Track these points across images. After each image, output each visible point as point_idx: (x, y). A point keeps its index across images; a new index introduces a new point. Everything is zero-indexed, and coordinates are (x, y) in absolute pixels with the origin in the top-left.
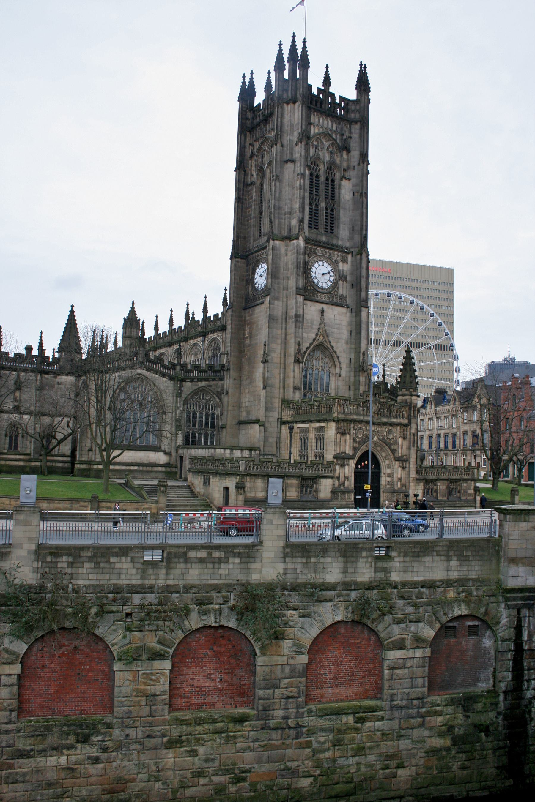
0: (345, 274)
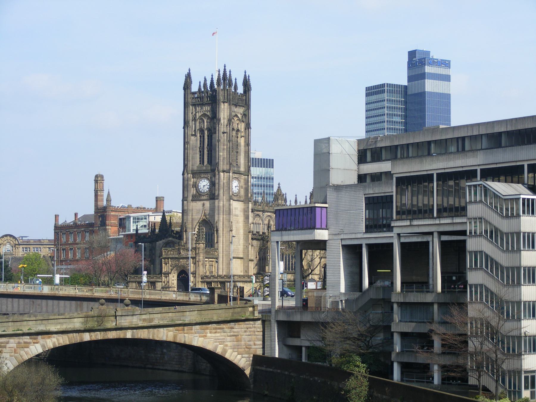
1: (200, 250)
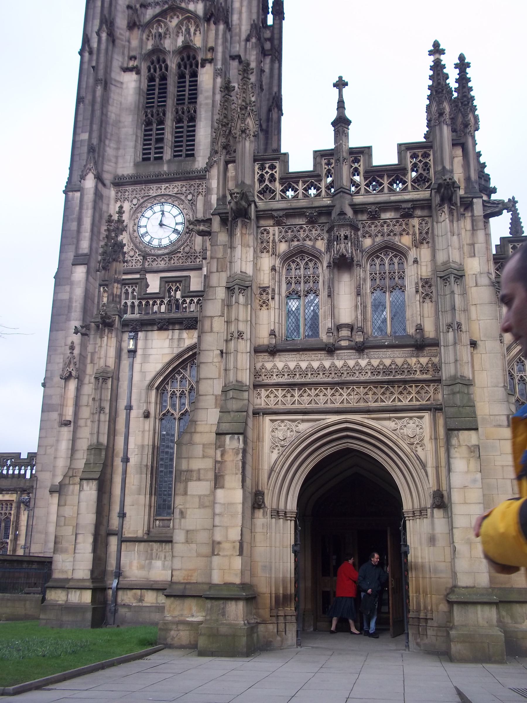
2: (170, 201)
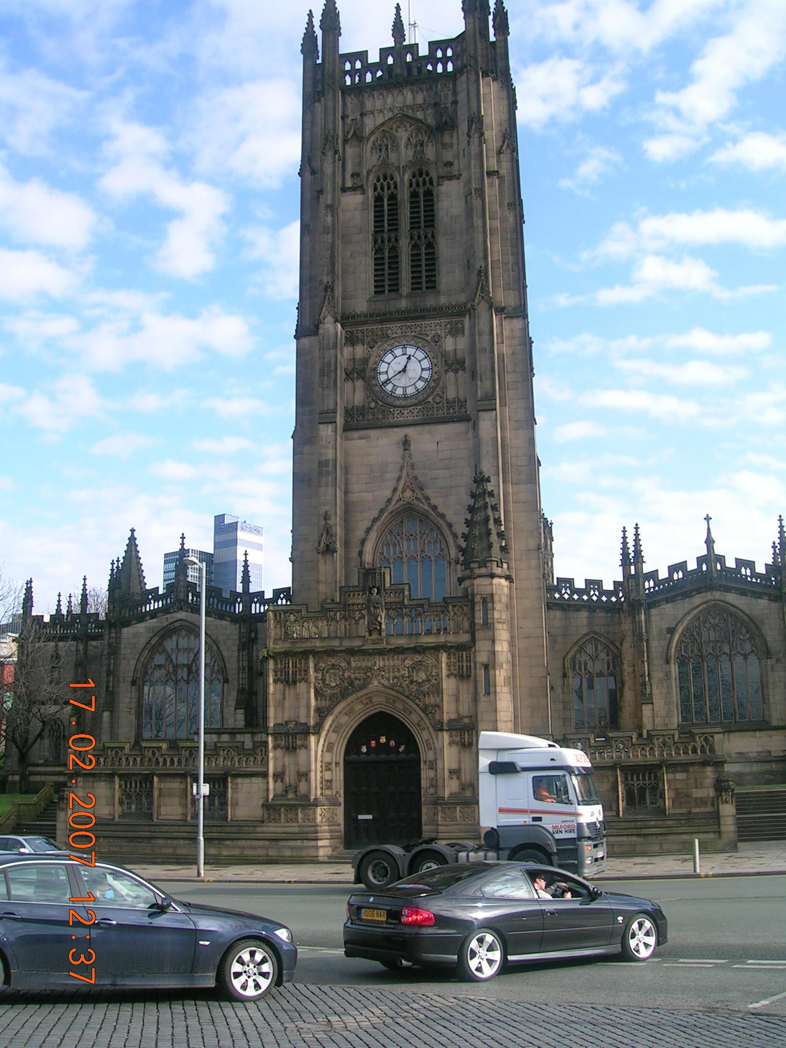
0: (459, 355)
1: (498, 606)
2: (413, 342)
